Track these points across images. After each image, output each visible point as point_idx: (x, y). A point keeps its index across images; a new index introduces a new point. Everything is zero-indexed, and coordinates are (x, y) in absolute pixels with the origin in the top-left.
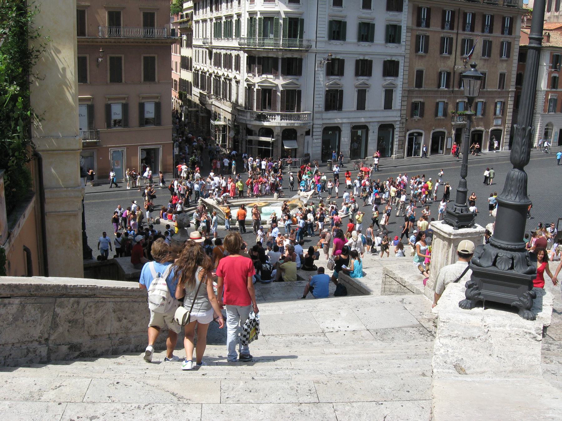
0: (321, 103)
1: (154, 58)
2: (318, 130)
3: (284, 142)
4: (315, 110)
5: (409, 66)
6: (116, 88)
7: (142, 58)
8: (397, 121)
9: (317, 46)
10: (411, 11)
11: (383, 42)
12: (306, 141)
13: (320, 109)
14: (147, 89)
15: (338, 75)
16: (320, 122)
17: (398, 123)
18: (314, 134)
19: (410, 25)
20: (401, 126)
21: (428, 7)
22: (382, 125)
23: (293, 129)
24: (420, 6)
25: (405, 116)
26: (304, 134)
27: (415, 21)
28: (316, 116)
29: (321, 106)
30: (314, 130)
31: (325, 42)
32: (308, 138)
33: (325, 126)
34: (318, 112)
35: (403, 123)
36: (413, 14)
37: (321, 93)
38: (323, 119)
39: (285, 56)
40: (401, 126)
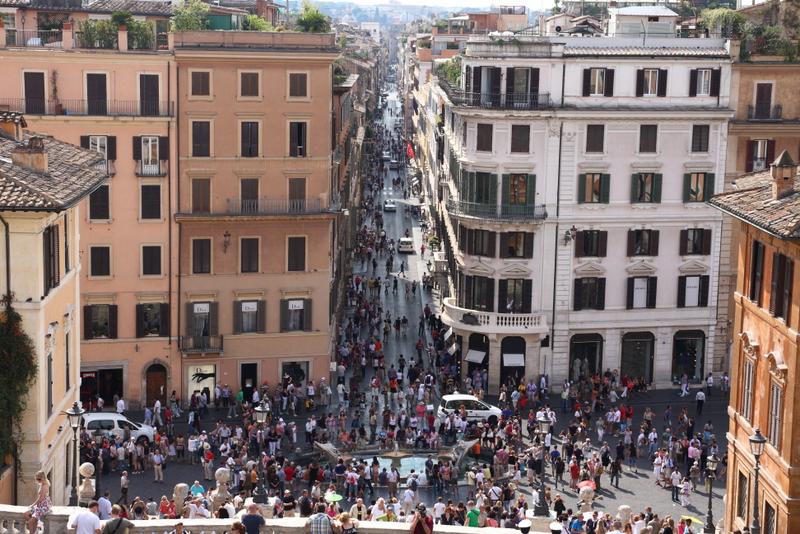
0: (566, 298)
1: (304, 239)
2: (563, 339)
3: (505, 356)
4: (557, 308)
5: (732, 237)
6: (250, 281)
7: (287, 240)
8: (709, 325)
9: (560, 214)
10: (734, 147)
11: (680, 201)
12: (542, 354)
13: (566, 308)
14: (294, 281)
15: (596, 255)
16: (566, 327)
17: (712, 328)
18: (555, 345)
19: (733, 170)
20: (719, 334)
21: (771, 139)
22: (680, 331)
23: (520, 337)
24: (752, 138)
25: (726, 317)
26: (539, 344)
27: (743, 164)
28: (559, 317)
29: (566, 303)
30: (555, 339)
31: (573, 206)
32: (546, 351)
33: (574, 333)
34: (562, 312)
35: (722, 329)
36: (738, 152)
37: (566, 283)
38: (569, 323)
39: (506, 231)
40: (719, 334)
